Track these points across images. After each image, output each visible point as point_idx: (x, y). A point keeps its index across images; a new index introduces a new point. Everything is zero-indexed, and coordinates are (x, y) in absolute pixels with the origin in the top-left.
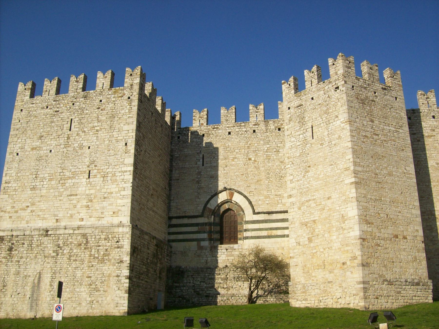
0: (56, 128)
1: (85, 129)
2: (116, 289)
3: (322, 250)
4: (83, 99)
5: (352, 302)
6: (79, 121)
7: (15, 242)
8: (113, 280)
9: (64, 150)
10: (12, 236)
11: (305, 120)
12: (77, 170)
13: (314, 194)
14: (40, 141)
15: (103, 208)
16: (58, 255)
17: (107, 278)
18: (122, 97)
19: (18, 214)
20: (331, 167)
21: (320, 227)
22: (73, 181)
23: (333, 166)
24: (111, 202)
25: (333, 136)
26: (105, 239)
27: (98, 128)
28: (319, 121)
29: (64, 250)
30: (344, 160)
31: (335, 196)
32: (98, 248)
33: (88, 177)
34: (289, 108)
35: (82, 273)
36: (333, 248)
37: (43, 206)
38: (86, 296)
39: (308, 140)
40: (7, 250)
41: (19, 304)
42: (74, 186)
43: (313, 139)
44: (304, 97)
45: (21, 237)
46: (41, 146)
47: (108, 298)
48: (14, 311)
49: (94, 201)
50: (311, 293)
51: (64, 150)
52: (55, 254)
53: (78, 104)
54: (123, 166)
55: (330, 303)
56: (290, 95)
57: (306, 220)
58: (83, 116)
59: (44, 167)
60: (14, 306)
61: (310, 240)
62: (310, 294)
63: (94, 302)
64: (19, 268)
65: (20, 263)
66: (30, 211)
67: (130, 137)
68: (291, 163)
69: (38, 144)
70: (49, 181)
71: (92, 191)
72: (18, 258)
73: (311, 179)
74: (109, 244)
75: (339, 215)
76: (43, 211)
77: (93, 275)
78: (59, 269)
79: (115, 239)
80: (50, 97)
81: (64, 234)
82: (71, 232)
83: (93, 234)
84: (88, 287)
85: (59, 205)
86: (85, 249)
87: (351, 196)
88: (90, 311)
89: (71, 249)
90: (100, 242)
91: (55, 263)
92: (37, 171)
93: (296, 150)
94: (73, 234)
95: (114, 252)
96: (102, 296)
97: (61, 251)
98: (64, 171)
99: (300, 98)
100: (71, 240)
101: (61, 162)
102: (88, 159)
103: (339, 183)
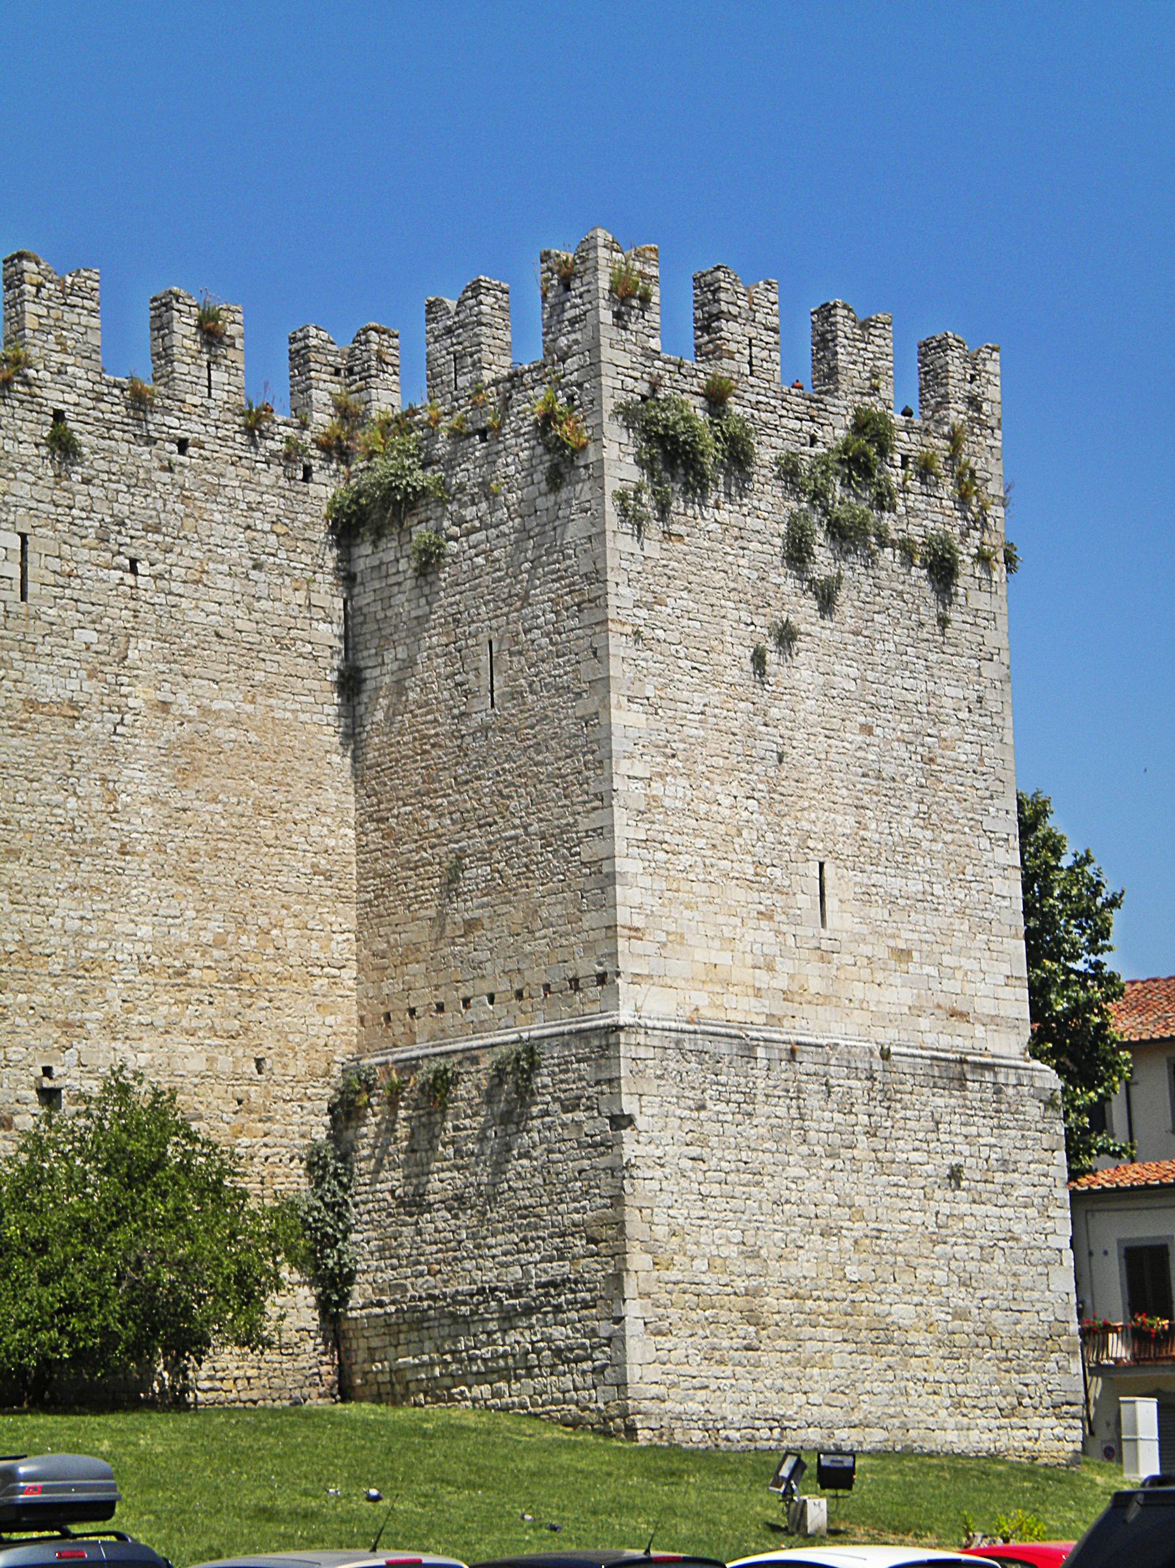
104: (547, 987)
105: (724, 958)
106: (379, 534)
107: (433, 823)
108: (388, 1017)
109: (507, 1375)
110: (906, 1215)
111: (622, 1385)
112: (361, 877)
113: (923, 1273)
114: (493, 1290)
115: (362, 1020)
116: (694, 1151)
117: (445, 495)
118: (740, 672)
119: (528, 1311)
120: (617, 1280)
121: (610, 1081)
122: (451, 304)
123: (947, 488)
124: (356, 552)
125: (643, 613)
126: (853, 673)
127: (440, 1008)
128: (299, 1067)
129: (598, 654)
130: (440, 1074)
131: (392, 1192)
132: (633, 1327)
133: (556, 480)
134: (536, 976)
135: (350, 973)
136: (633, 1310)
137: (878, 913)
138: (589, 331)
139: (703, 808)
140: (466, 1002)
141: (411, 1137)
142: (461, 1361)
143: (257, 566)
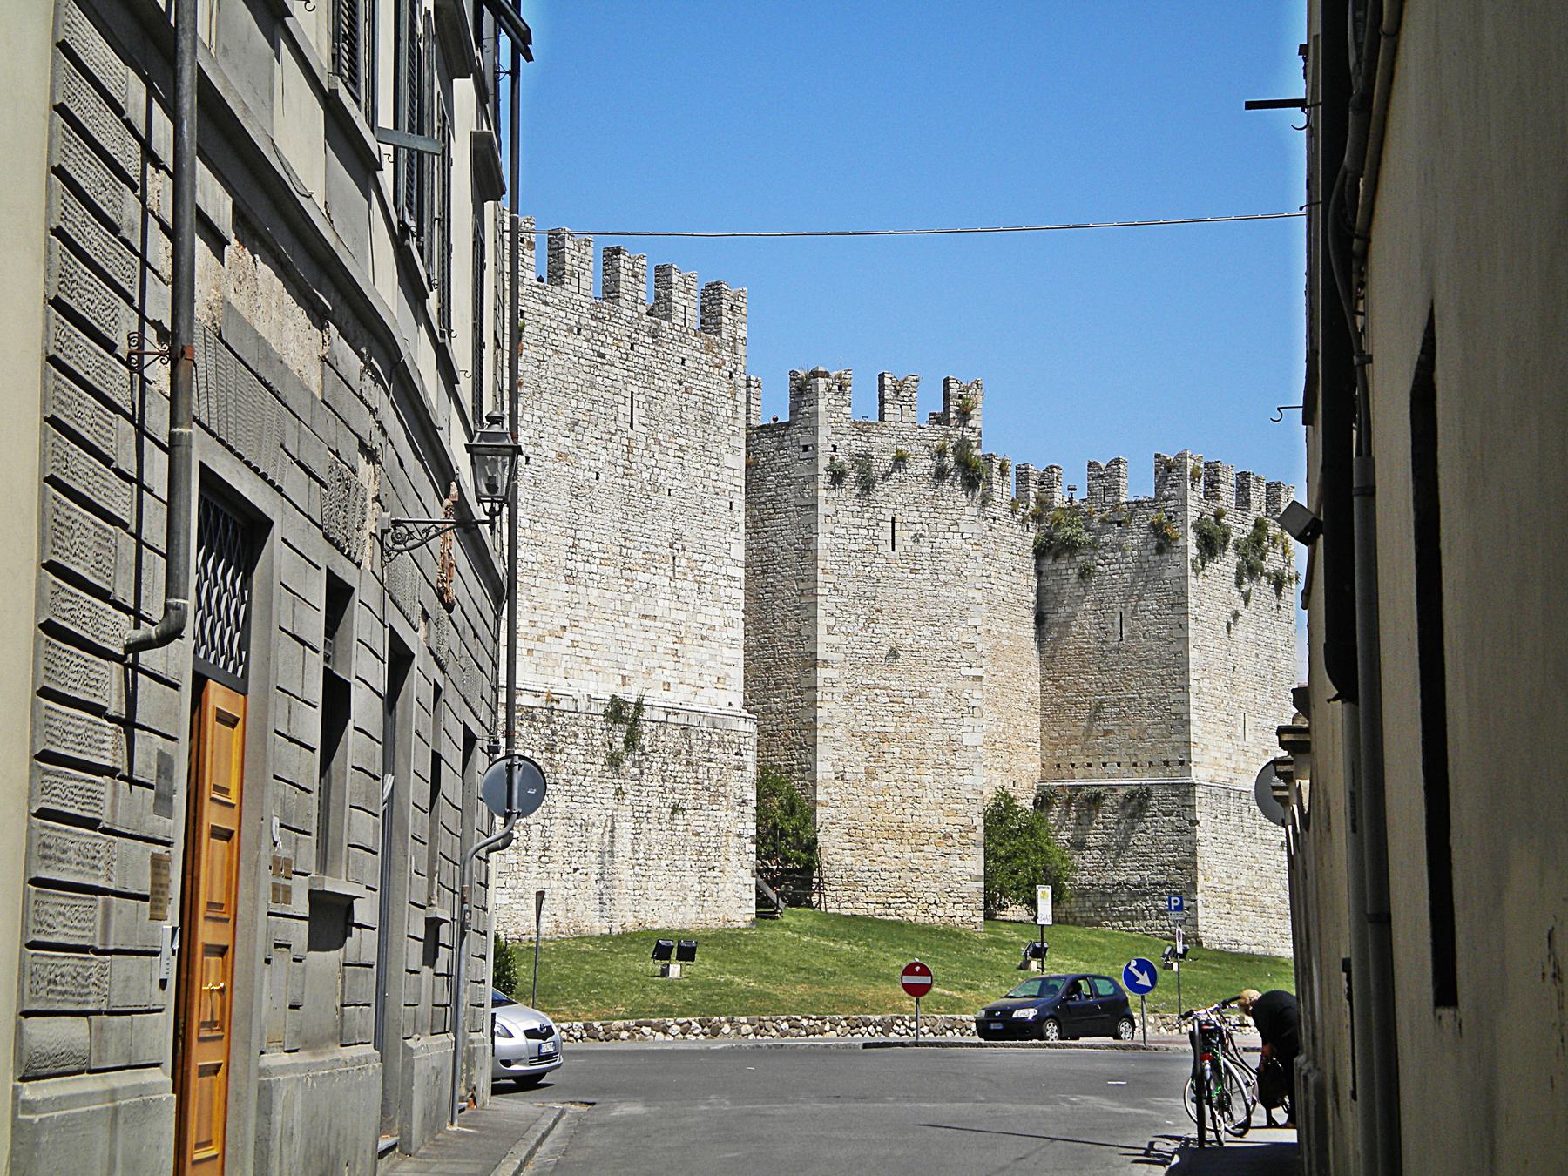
0: (603, 410)
1: (660, 436)
2: (739, 866)
3: (897, 799)
4: (649, 340)
5: (960, 913)
6: (646, 406)
7: (558, 727)
8: (734, 841)
9: (626, 482)
10: (552, 709)
11: (877, 498)
12: (652, 549)
13: (888, 675)
14: (573, 434)
15: (702, 664)
16: (642, 773)
17: (724, 839)
18: (720, 368)
19: (545, 647)
20: (931, 628)
21: (897, 750)
22: (647, 577)
23: (936, 628)
24: (713, 652)
25: (943, 563)
26: (719, 746)
27: (682, 441)
28: (911, 514)
29: (652, 762)
30: (964, 625)
31: (937, 695)
32: (708, 764)
33: (671, 574)
34: (835, 448)
35: (685, 822)
36: (925, 800)
37: (596, 634)
38: (693, 879)
39: (880, 548)
40: (543, 748)
41: (578, 897)
42: (649, 593)
43: (893, 550)
44: (878, 440)
45: (570, 714)
46: (576, 451)
47: (728, 886)
48: (570, 915)
49: (685, 640)
50: (867, 886)
51: (626, 482)
52: (637, 771)
53: (642, 350)
54: (727, 562)
55: (914, 912)
56: (840, 415)
57: (863, 728)
58: (654, 394)
59: (588, 520)
60: (569, 901)
61: (870, 774)
62: (864, 889)
63: (707, 894)
64: (572, 801)
65: (573, 788)
66: (569, 644)
67: (738, 489)
68: (831, 586)
69: (569, 442)
70: (601, 564)
71: (681, 616)
72: (567, 774)
73: (883, 640)
74: (725, 757)
75: (943, 735)
76: (595, 648)
77: (702, 829)
78: (646, 809)
79: (734, 745)
80: (582, 298)
81: (650, 721)
82: (663, 718)
83: (699, 729)
84: (695, 858)
85: (625, 638)
86: (688, 763)
87: (972, 703)
88: (702, 916)
89: (665, 763)
90: (711, 750)
91: (638, 794)
92: (574, 526)
93: (846, 559)
94: (667, 722)
95: (733, 779)
96: (717, 880)
97: (646, 764)
98: (628, 544)
99: (868, 438)
100: (663, 738)
101: (620, 514)
102: (670, 522)
103: (947, 669)
104: (1151, 763)
105: (1218, 755)
106: (1056, 557)
107: (1086, 686)
108: (1059, 766)
109: (1132, 919)
110: (1269, 861)
111: (1195, 926)
112: (1042, 704)
113: (1273, 884)
114: (1125, 884)
115: (1043, 766)
116: (1214, 835)
117: (1093, 545)
118: (1222, 633)
119: (1144, 894)
120: (1194, 885)
121: (1189, 806)
122: (1103, 465)
123: (1280, 550)
124: (1042, 562)
125: (1197, 609)
126: (1254, 631)
127: (1089, 765)
128: (1025, 785)
129: (1184, 627)
130: (1098, 795)
131: (1068, 840)
132: (1200, 904)
133: (1160, 550)
134: (1146, 758)
135: (1038, 745)
136: (1199, 897)
137: (1259, 734)
138: (1181, 491)
139: (1213, 691)
140: (1104, 765)
141: (1078, 818)
142: (1106, 912)
143: (1014, 570)
